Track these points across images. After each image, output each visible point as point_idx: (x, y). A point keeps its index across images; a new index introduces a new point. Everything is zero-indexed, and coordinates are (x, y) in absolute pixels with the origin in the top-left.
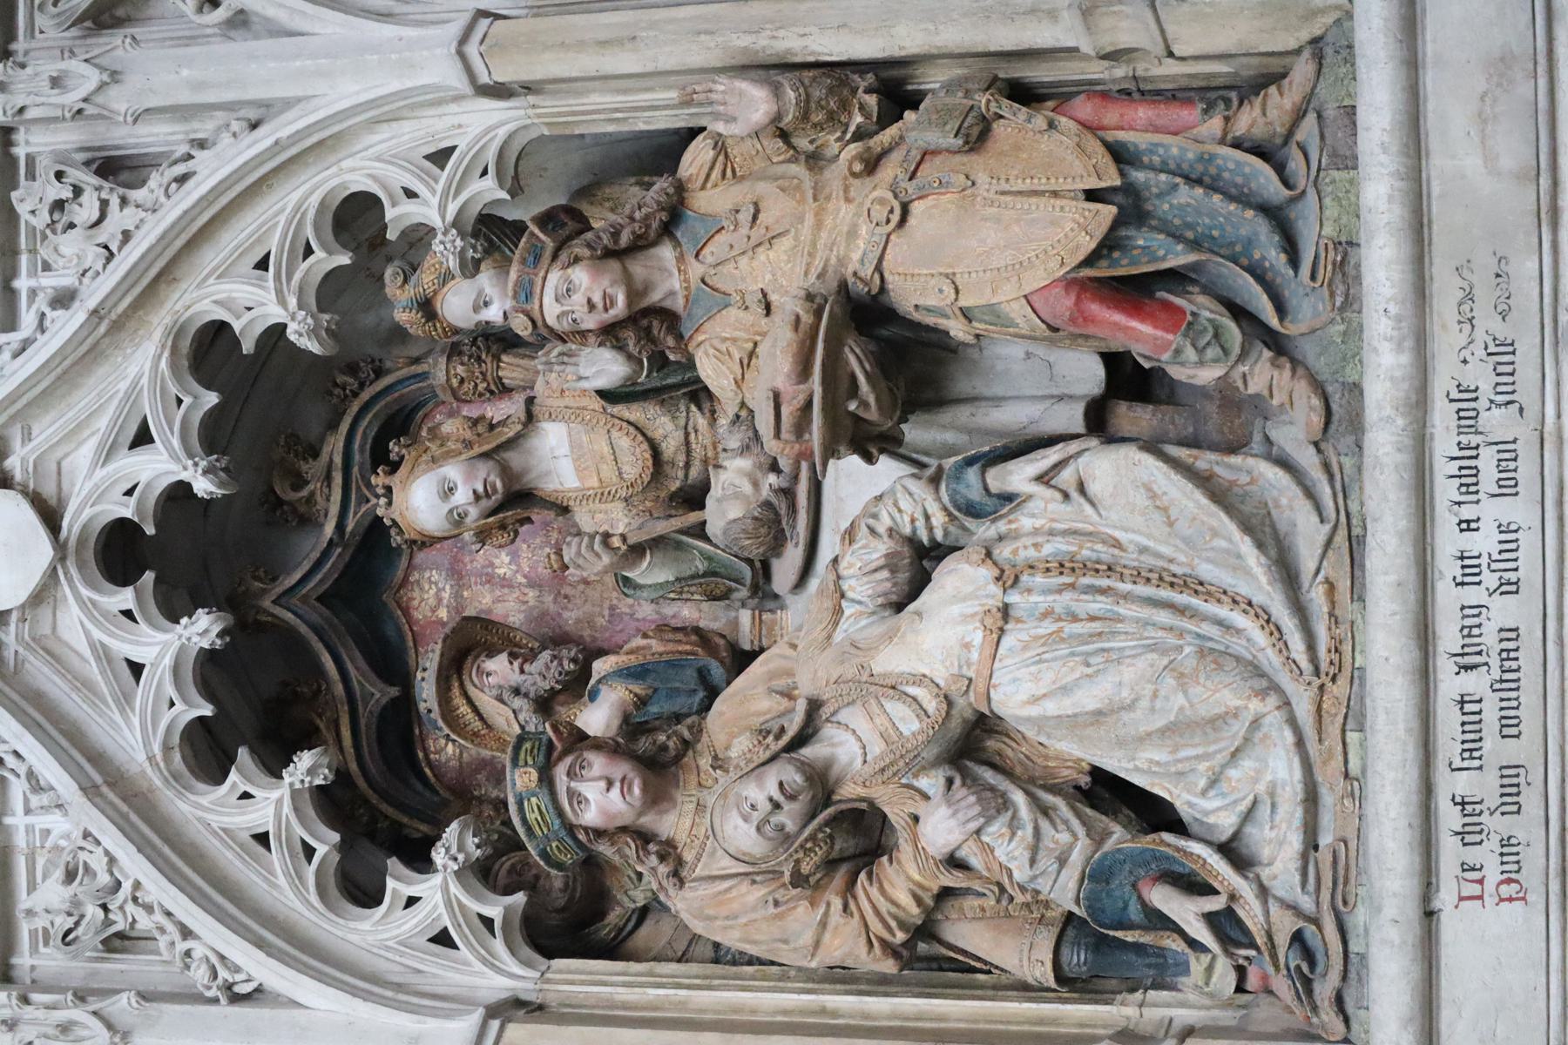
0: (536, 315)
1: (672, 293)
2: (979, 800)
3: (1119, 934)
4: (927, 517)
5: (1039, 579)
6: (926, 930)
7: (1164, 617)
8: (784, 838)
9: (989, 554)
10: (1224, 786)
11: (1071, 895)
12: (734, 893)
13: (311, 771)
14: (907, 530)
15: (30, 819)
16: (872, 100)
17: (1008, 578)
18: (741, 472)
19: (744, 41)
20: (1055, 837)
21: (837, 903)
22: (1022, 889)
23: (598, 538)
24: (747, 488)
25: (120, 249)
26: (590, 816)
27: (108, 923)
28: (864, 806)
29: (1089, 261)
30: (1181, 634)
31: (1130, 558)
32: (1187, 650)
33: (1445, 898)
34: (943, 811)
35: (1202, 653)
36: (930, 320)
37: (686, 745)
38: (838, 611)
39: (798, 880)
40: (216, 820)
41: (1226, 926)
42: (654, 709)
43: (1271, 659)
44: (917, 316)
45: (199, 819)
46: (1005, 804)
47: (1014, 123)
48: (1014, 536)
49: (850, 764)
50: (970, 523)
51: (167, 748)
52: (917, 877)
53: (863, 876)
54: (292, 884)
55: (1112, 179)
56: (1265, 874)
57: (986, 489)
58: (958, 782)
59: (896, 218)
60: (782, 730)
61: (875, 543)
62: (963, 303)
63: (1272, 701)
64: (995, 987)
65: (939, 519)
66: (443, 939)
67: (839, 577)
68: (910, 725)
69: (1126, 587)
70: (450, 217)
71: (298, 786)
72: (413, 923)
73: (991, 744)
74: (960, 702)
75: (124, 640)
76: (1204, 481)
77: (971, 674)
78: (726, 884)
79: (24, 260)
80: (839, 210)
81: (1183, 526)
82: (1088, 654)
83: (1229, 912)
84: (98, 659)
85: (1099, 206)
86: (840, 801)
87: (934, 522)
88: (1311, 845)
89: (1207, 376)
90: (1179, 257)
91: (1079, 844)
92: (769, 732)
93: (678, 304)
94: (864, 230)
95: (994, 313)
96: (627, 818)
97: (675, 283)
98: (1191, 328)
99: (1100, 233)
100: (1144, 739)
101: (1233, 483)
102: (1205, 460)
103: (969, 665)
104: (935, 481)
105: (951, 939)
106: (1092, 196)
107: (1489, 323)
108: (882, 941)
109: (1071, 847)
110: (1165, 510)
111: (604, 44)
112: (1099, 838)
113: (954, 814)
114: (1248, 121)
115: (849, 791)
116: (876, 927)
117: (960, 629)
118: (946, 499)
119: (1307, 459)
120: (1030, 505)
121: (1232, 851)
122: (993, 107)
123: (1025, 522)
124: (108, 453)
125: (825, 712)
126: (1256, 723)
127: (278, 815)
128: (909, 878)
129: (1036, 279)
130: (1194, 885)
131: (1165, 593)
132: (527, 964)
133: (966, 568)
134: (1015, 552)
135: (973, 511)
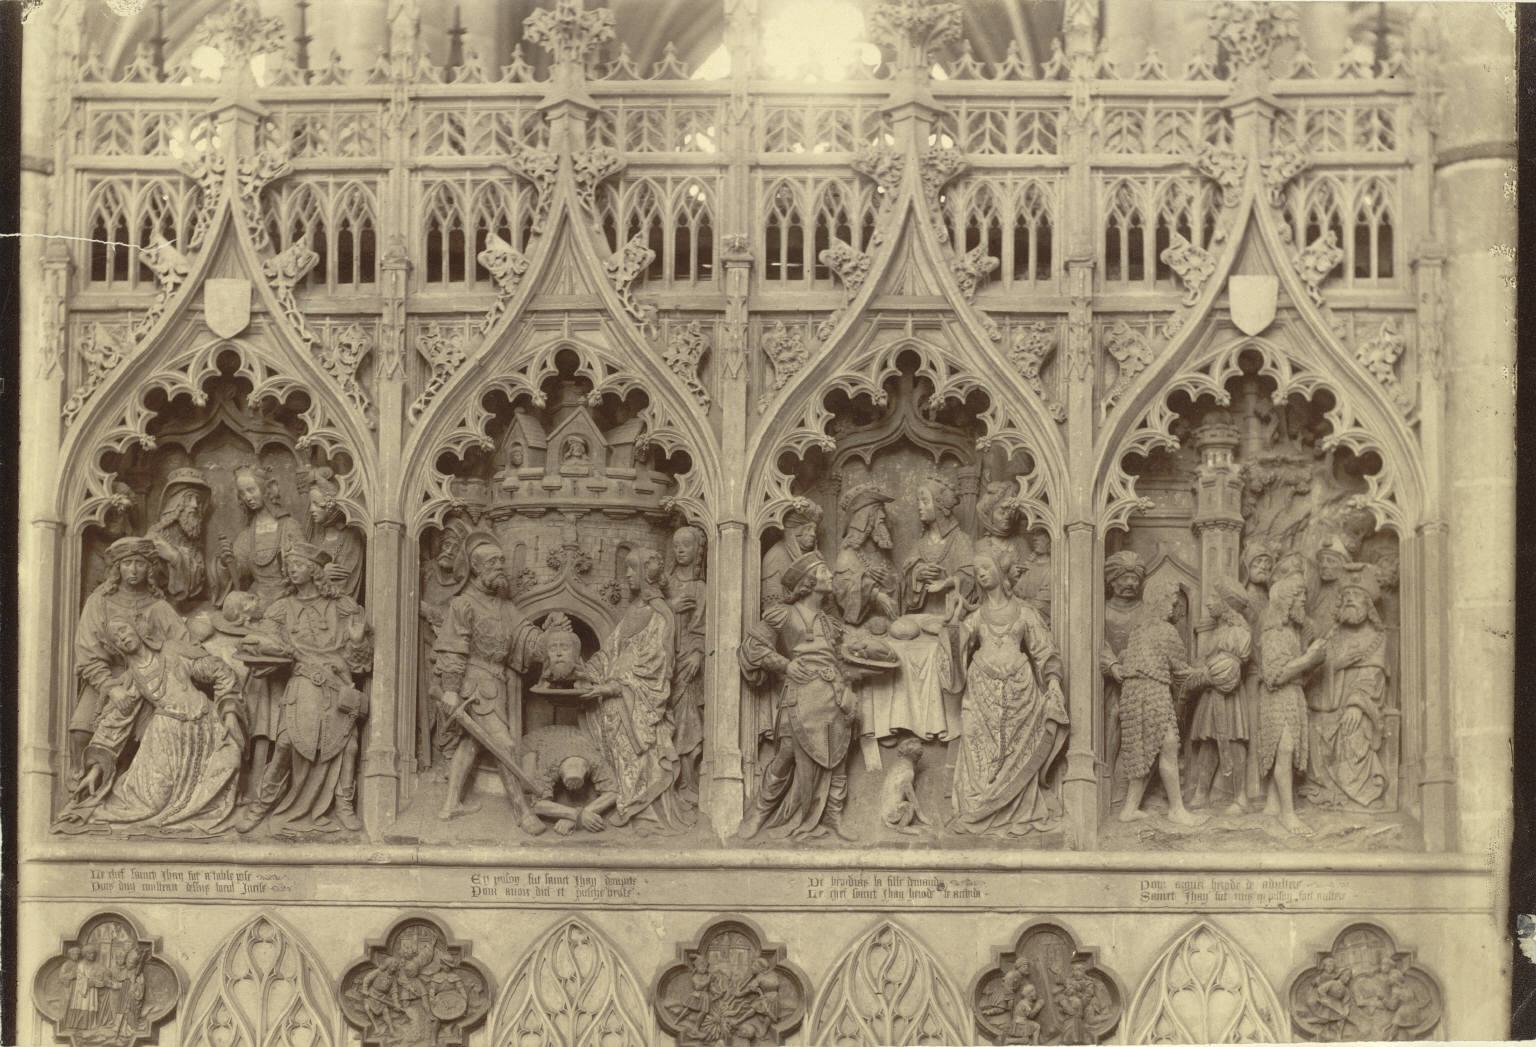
7: (183, 773)
16: (359, 671)
17: (198, 720)
33: (92, 866)
35: (171, 787)
41: (84, 794)
46: (127, 715)
47: (346, 724)
76: (226, 787)
83: (88, 794)
90: (298, 779)
102: (233, 787)
106: (318, 752)
107: (270, 884)
112: (114, 749)
114: (343, 804)
119: (231, 823)
130: (99, 783)
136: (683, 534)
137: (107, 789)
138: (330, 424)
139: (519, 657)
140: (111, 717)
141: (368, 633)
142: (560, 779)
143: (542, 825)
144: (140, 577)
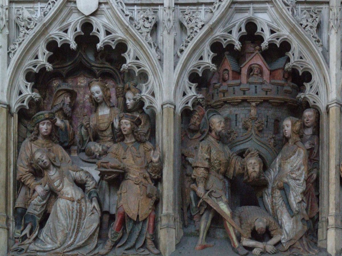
0: (123, 118)
1: (127, 141)
2: (44, 196)
3: (23, 219)
4: (89, 187)
5: (79, 206)
6: (23, 184)
7: (73, 227)
8: (37, 162)
9: (82, 198)
10: (46, 237)
11: (29, 211)
12: (29, 151)
13: (48, 68)
14: (87, 183)
15: (39, 8)
16: (156, 177)
17: (79, 201)
18: (99, 149)
19: (166, 156)
20: (38, 208)
21: (28, 170)
22: (30, 203)
23: (88, 122)
24: (96, 150)
25: (139, 32)
26: (41, 126)
27: (21, 26)
28: (43, 176)
29: (128, 216)
30: (70, 230)
31: (82, 222)
32: (67, 232)
34: (42, 190)
35: (67, 234)
36: (120, 188)
37: (53, 141)
38: (74, 171)
39: (31, 164)
40: (40, 48)
41: (25, 237)
42: (60, 132)
43: (66, 245)
44: (121, 185)
45: (40, 45)
46: (44, 199)
47: (151, 202)
48: (86, 202)
49: (50, 173)
50: (88, 193)
51: (52, 38)
52: (32, 184)
53: (32, 174)
54: (28, 64)
55: (140, 220)
56: (33, 244)
57: (93, 197)
58: (47, 192)
59: (136, 183)
60: (55, 161)
61: (85, 177)
62: (122, 194)
63: (59, 245)
64: (15, 195)
65: (88, 189)
66: (20, 93)
67: (80, 171)
68: (56, 184)
69: (77, 221)
70: (143, 97)
71: (46, 65)
72: (23, 88)
73: (54, 196)
74: (59, 193)
75: (71, 30)
76: (93, 234)
77: (64, 195)
78: (30, 150)
79: (140, 8)
80: (138, 172)
81: (86, 231)
82: (67, 215)
84: (68, 24)
85: (136, 218)
86: (43, 171)
87: (88, 188)
88: (38, 251)
89: (109, 236)
90: (128, 230)
91: (37, 212)
92: (55, 159)
93: (125, 142)
94: (134, 177)
95: (120, 199)
96: (40, 132)
97: (128, 142)
98: (116, 233)
99: (132, 218)
100: (53, 223)
101: (93, 238)
102: (97, 234)
103: (65, 195)
104: (95, 188)
105: (23, 188)
106: (138, 216)
108: (22, 178)
109: (37, 211)
110: (89, 228)
111: (168, 130)
113: (42, 192)
115: (46, 173)
116: (24, 177)
117: (71, 193)
118: (91, 190)
119: (96, 252)
120: (90, 205)
121: (37, 238)
122: (153, 199)
123: (88, 204)
124: (104, 26)
125: (58, 168)
126: (56, 243)
127: (41, 61)
128: (31, 183)
129: (125, 207)
130: (31, 232)
131: (76, 227)
132: (17, 109)
133: (80, 195)
134: (83, 202)
135: (90, 195)
136: (308, 113)
137: (34, 236)
138: (137, 59)
139: (231, 171)
140: (36, 200)
141: (161, 161)
142: (254, 228)
143: (246, 251)
144: (49, 131)
